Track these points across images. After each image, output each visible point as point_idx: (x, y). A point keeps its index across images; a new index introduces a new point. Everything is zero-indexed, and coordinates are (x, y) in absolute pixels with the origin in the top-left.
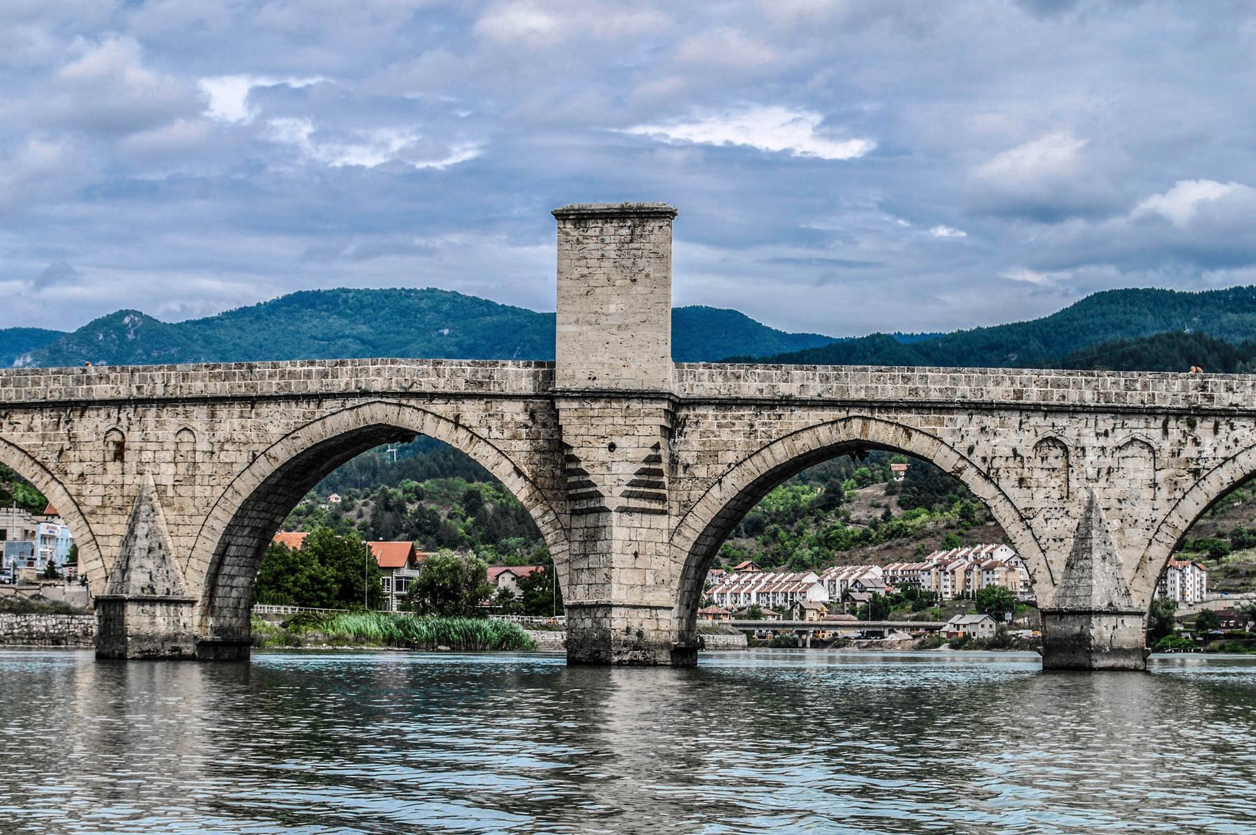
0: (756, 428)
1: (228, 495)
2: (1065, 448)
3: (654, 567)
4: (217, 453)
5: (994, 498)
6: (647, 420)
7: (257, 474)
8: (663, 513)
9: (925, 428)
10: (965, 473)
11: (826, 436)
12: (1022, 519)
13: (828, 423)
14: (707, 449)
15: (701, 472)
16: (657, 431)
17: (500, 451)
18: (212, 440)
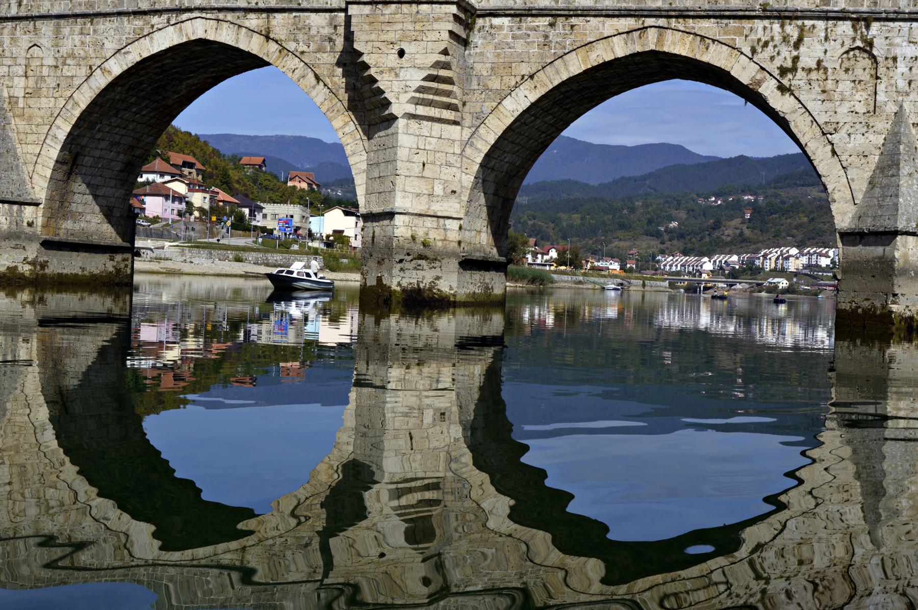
0: (551, 38)
1: (69, 106)
2: (874, 58)
3: (443, 177)
4: (61, 67)
5: (794, 112)
6: (436, 26)
7: (94, 87)
8: (456, 123)
9: (722, 38)
10: (764, 86)
11: (620, 49)
12: (824, 134)
13: (623, 33)
14: (501, 60)
15: (495, 84)
16: (446, 36)
17: (306, 64)
18: (57, 56)
